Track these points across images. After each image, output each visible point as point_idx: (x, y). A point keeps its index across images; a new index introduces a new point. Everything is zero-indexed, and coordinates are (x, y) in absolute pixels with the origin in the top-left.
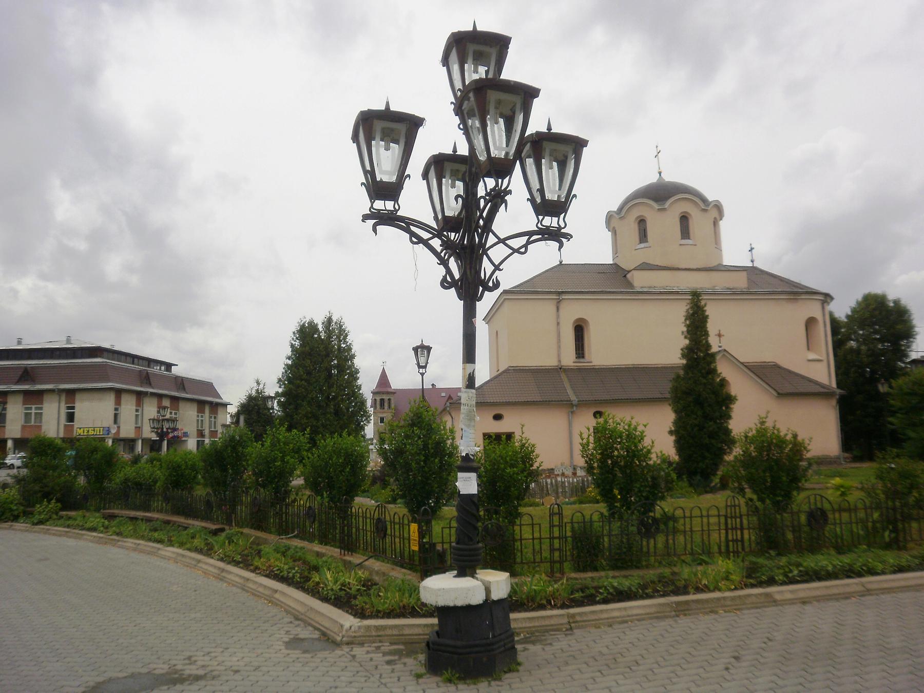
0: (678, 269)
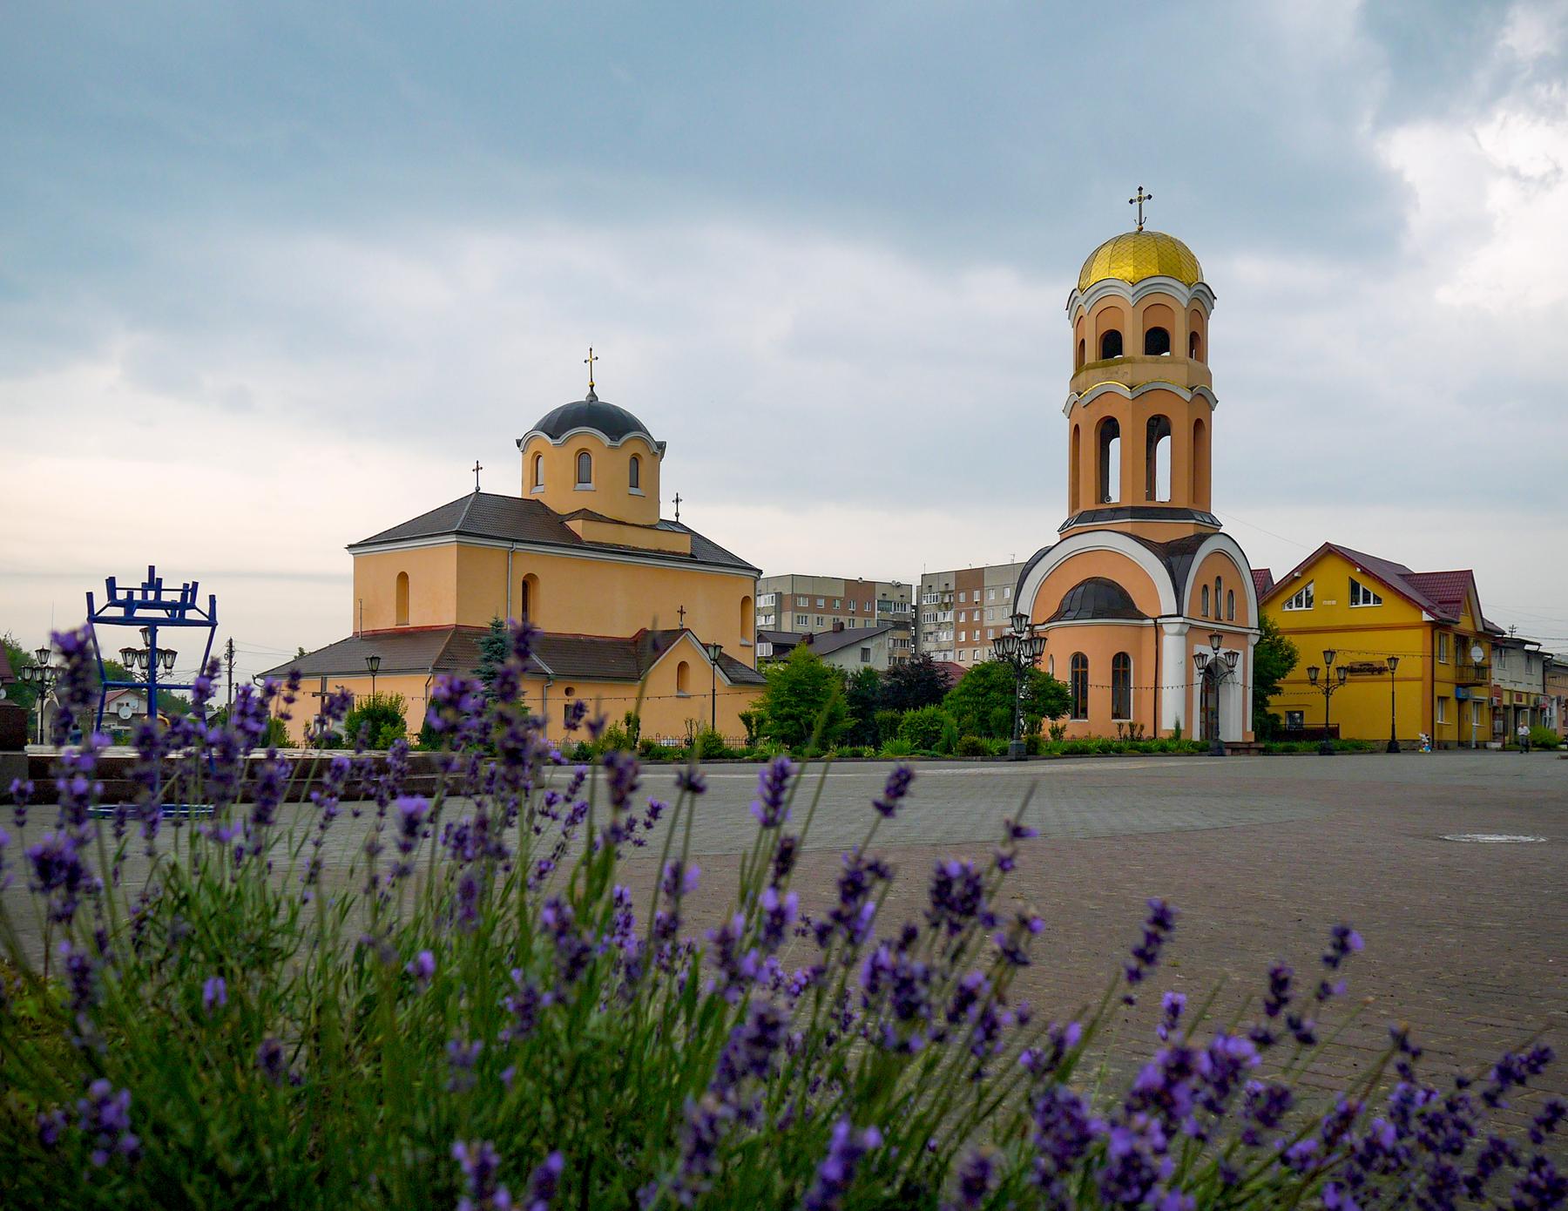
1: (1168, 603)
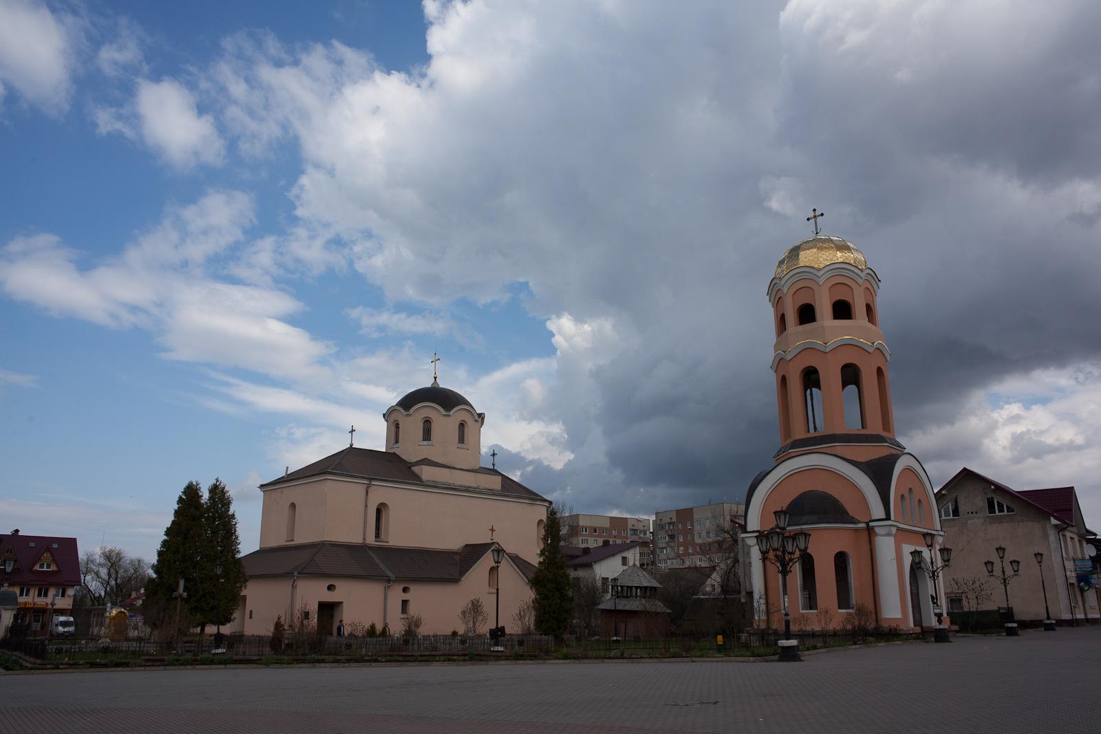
0: (454, 468)
1: (877, 511)
